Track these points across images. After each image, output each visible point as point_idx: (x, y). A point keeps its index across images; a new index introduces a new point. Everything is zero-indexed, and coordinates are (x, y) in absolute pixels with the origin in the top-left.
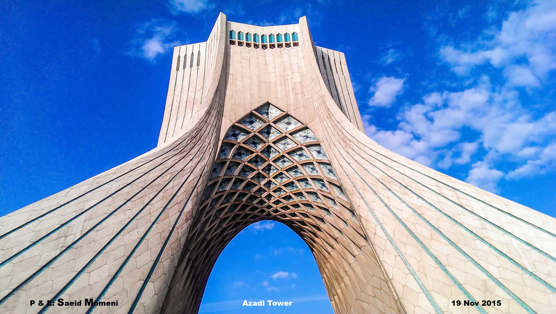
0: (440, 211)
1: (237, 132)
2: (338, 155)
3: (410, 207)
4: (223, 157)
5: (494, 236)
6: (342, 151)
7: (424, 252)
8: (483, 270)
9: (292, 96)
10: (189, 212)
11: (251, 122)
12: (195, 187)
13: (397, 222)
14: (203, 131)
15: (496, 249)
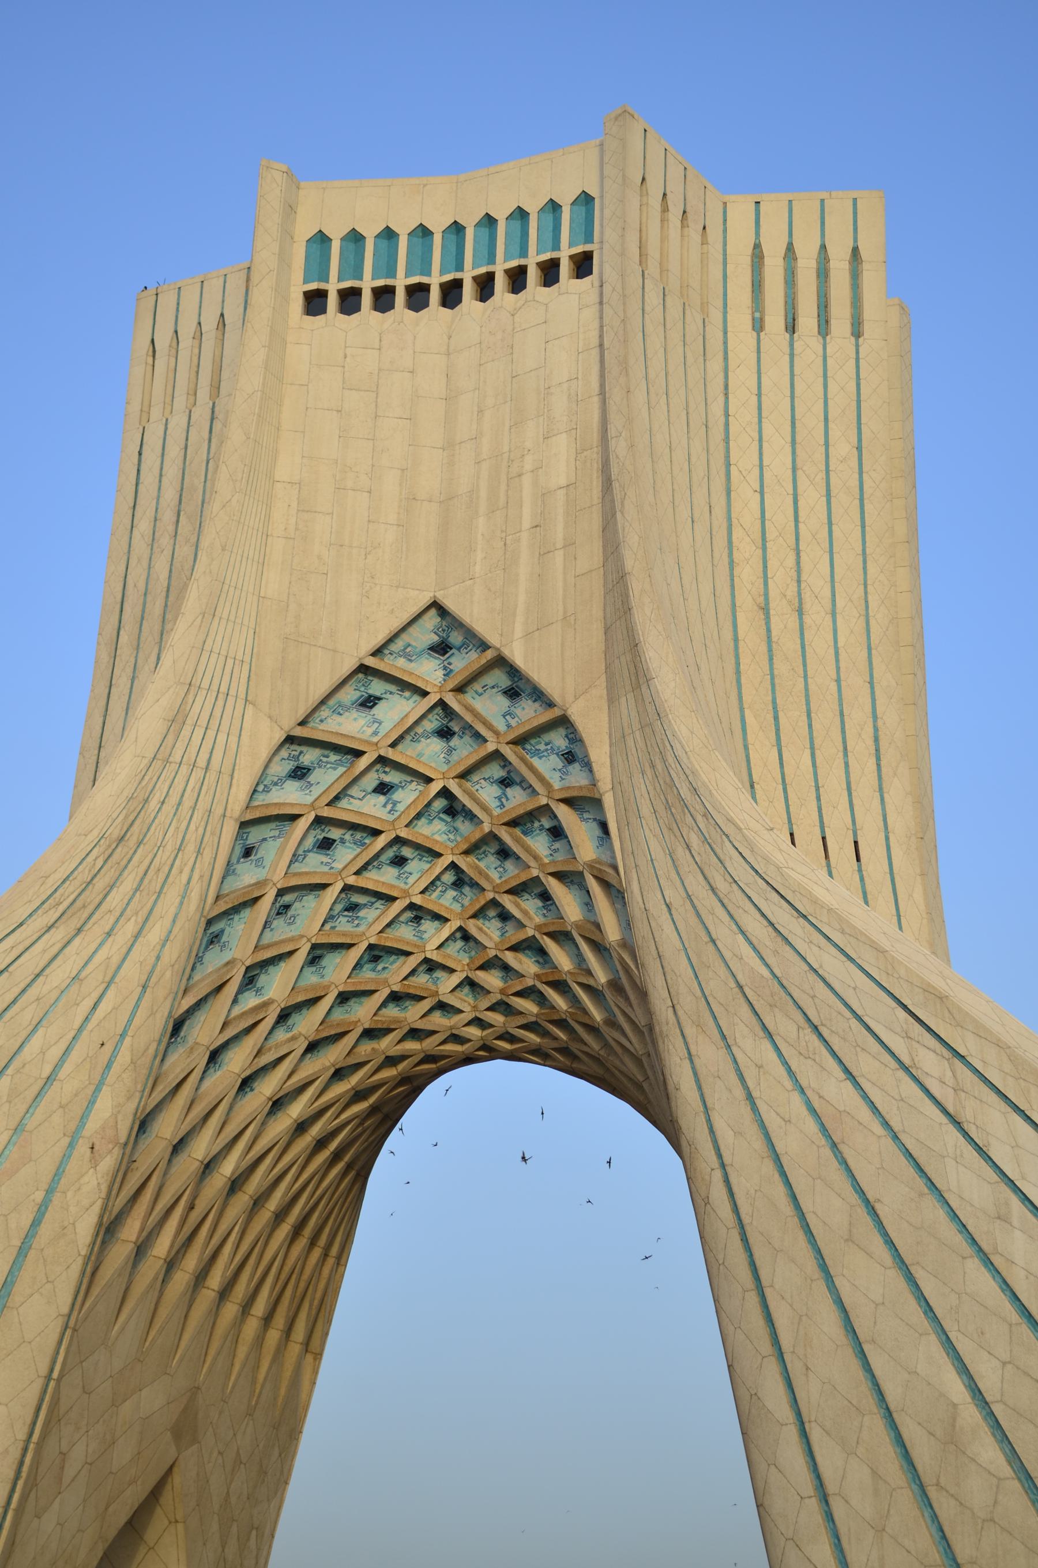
0: (895, 1137)
3: (813, 1111)
4: (247, 875)
7: (821, 1286)
9: (524, 569)
10: (103, 1128)
11: (369, 702)
12: (123, 1035)
13: (768, 1168)
14: (154, 804)
15: (1015, 1297)
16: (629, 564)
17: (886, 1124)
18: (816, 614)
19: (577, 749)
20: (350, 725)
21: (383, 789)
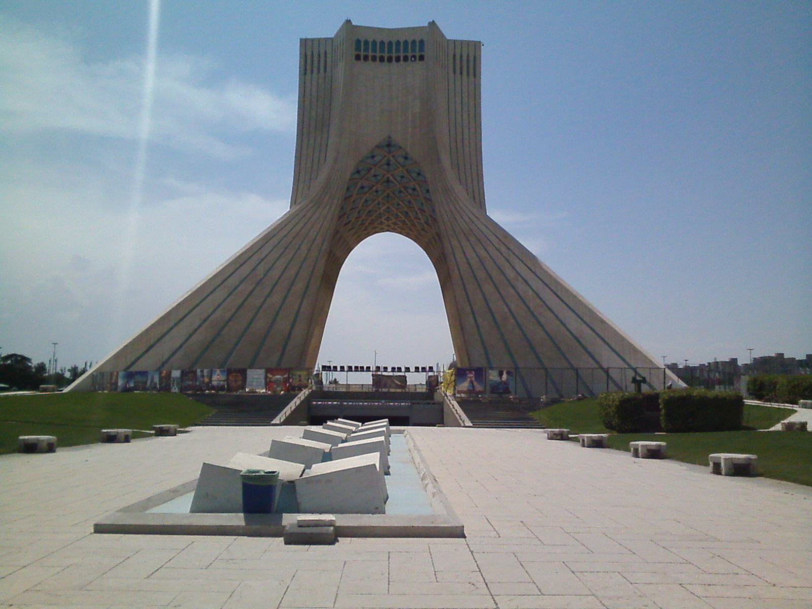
5: (520, 286)
8: (507, 306)
11: (373, 157)
15: (518, 293)
18: (466, 142)
21: (375, 176)
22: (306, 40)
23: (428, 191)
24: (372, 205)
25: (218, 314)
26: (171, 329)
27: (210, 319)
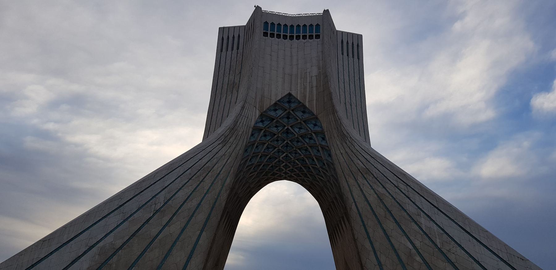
0: (395, 199)
1: (264, 119)
2: (335, 146)
3: (376, 193)
4: (252, 140)
5: (423, 221)
6: (338, 143)
13: (366, 203)
16: (332, 91)
17: (392, 196)
19: (318, 124)
20: (272, 114)
21: (276, 127)
22: (224, 28)
23: (324, 139)
24: (273, 152)
25: (109, 239)
26: (51, 253)
27: (97, 246)
